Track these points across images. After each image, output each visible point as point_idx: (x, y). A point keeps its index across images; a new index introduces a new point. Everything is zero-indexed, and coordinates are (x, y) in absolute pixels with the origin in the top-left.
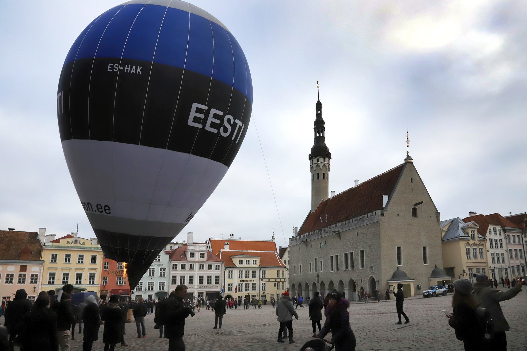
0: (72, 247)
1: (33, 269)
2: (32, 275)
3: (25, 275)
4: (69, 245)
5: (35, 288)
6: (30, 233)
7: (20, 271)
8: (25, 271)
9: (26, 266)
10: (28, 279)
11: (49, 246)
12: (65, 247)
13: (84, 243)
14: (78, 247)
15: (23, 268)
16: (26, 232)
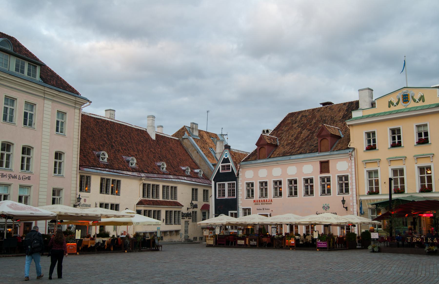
0: (397, 112)
1: (340, 165)
2: (340, 178)
3: (329, 179)
4: (393, 108)
5: (343, 201)
6: (351, 103)
7: (321, 172)
8: (328, 172)
9: (327, 162)
10: (334, 186)
11: (357, 119)
12: (384, 114)
13: (422, 98)
14: (410, 110)
15: (324, 166)
16: (345, 104)
